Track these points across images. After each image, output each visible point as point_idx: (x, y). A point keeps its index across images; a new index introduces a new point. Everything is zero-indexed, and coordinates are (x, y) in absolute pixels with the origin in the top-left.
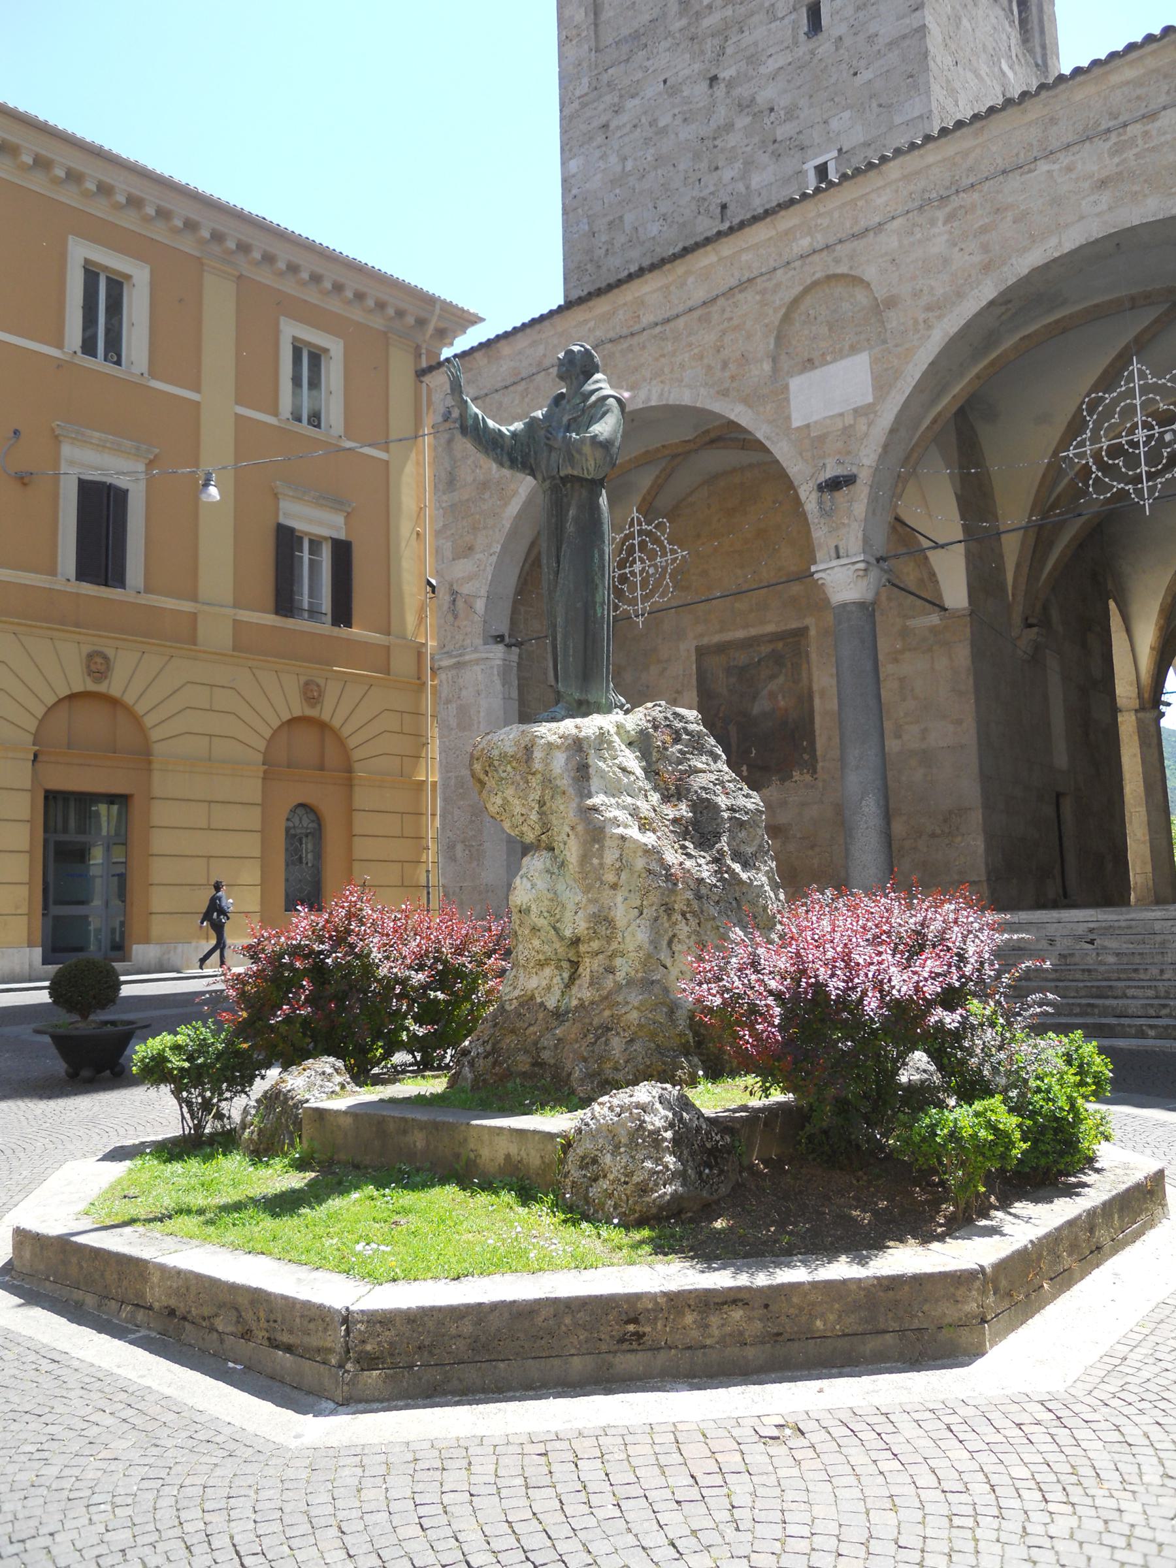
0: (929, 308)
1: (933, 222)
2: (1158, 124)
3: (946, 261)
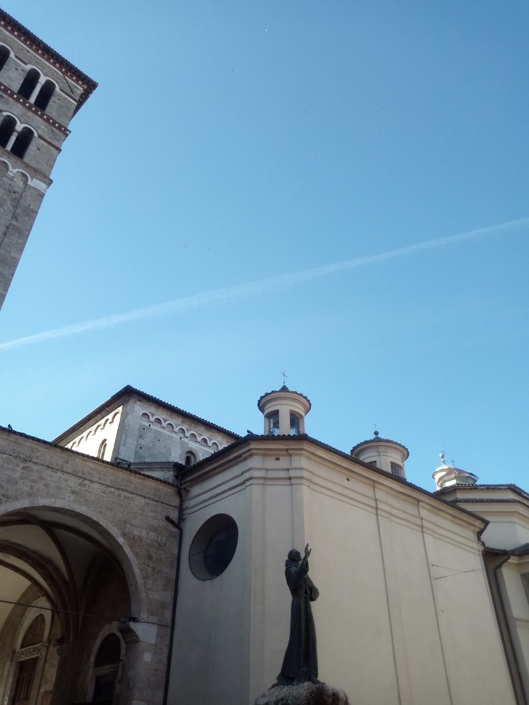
0: (4, 495)
1: (18, 465)
2: (93, 485)
3: (17, 482)
